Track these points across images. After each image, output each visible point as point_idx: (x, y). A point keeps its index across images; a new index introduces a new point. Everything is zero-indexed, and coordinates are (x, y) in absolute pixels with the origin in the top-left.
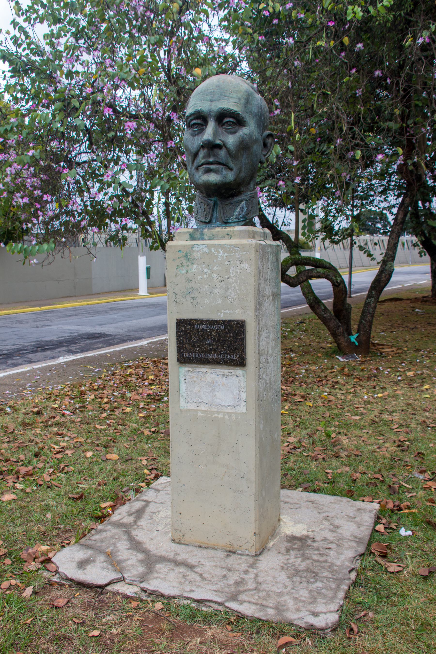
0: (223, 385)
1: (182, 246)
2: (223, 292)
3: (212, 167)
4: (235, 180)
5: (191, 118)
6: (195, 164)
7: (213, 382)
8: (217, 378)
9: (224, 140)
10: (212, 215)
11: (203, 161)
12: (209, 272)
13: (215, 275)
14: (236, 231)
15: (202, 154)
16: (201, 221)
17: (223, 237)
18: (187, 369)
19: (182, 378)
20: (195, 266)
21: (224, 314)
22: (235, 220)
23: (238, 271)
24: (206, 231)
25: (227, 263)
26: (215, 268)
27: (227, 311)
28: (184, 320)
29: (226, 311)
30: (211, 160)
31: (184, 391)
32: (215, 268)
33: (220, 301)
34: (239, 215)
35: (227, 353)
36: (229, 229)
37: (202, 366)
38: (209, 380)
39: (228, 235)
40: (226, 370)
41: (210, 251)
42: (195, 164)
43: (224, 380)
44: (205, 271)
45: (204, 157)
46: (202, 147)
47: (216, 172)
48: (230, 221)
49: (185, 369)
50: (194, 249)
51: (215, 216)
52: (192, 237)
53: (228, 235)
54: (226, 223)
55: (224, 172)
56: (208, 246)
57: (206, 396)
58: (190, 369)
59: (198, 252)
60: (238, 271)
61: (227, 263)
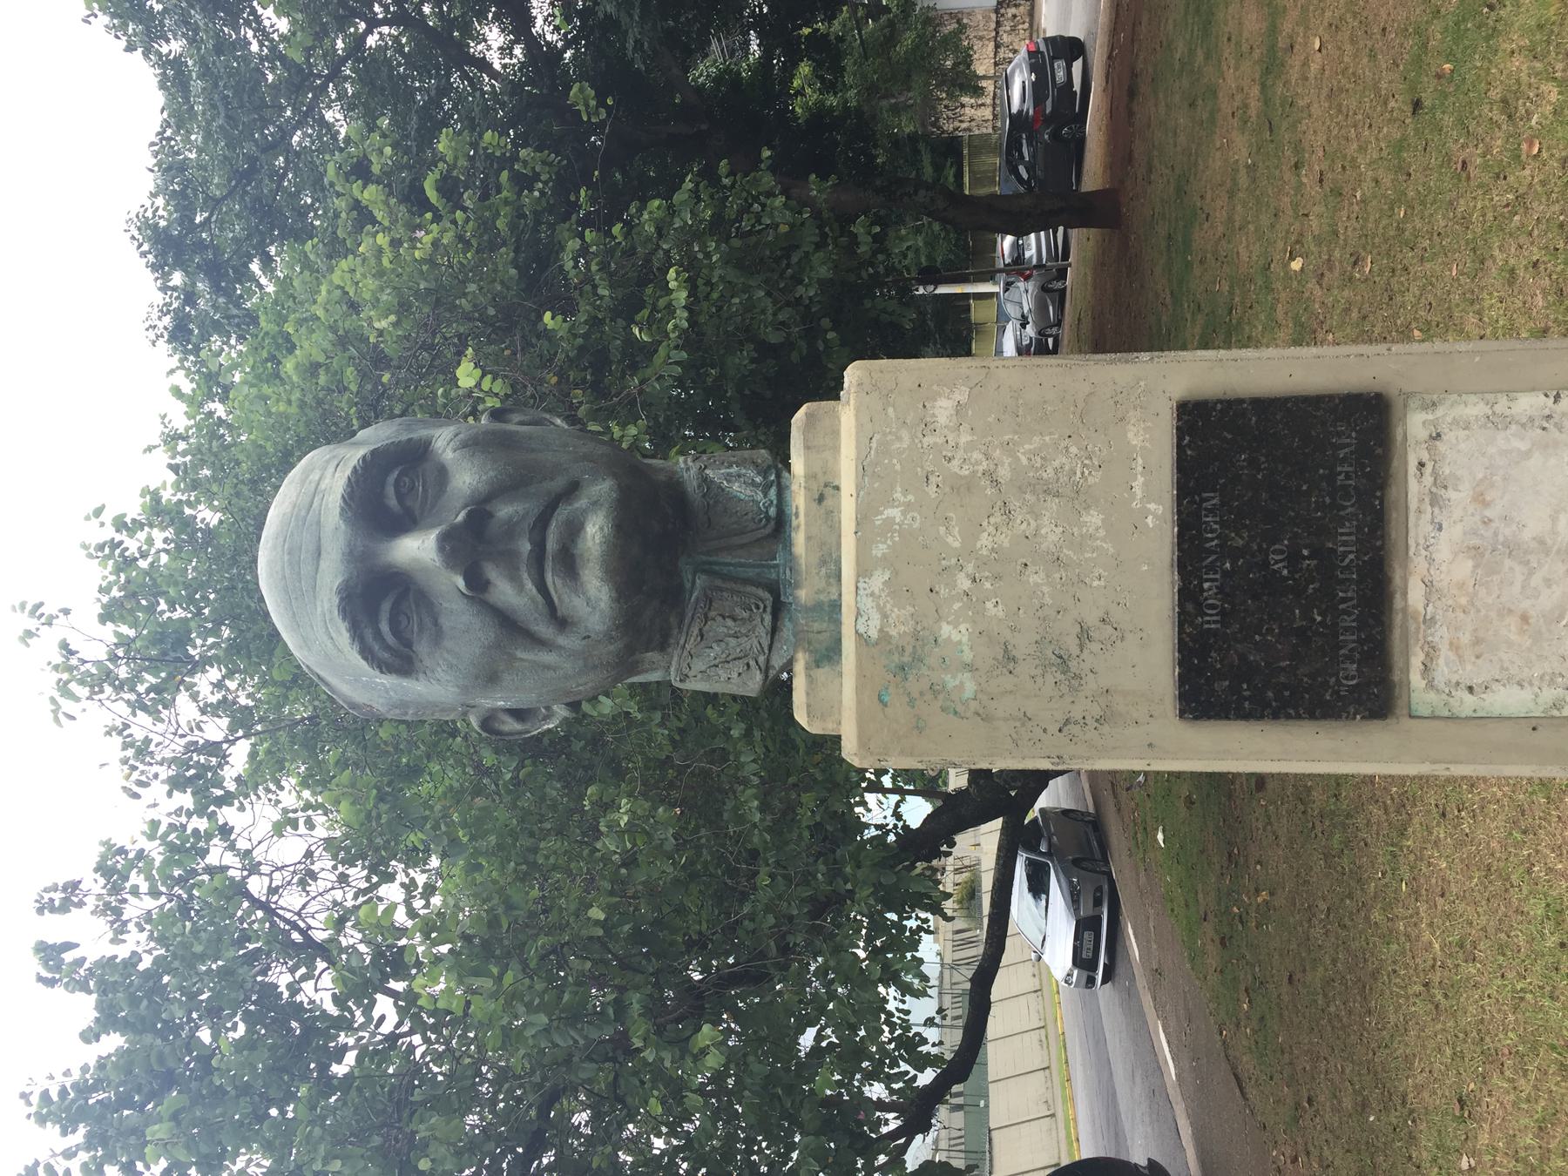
0: (1480, 499)
1: (859, 689)
2: (1053, 504)
3: (552, 544)
4: (615, 476)
5: (368, 634)
6: (544, 630)
7: (1475, 551)
8: (1453, 533)
9: (459, 505)
10: (747, 581)
11: (529, 586)
12: (970, 568)
13: (985, 541)
14: (807, 465)
15: (507, 592)
16: (774, 631)
17: (831, 520)
18: (1416, 679)
19: (1466, 704)
20: (946, 630)
21: (1148, 498)
22: (773, 492)
23: (965, 438)
24: (803, 595)
25: (932, 489)
26: (955, 542)
27: (1138, 483)
28: (1182, 680)
29: (1138, 491)
30: (525, 547)
31: (1526, 695)
32: (955, 542)
33: (1094, 519)
34: (753, 484)
35: (1331, 478)
36: (799, 499)
37: (1398, 603)
38: (1464, 568)
39: (821, 499)
40: (1415, 488)
41: (885, 561)
42: (544, 630)
43: (1458, 497)
44: (965, 584)
45: (515, 579)
46: (477, 585)
47: (574, 529)
48: (772, 511)
49: (1418, 688)
50: (874, 634)
51: (751, 573)
52: (829, 654)
53: (821, 499)
54: (780, 525)
55: (582, 503)
56: (863, 572)
57: (1548, 582)
58: (1417, 661)
59: (885, 616)
60: (965, 438)
61: (932, 489)
